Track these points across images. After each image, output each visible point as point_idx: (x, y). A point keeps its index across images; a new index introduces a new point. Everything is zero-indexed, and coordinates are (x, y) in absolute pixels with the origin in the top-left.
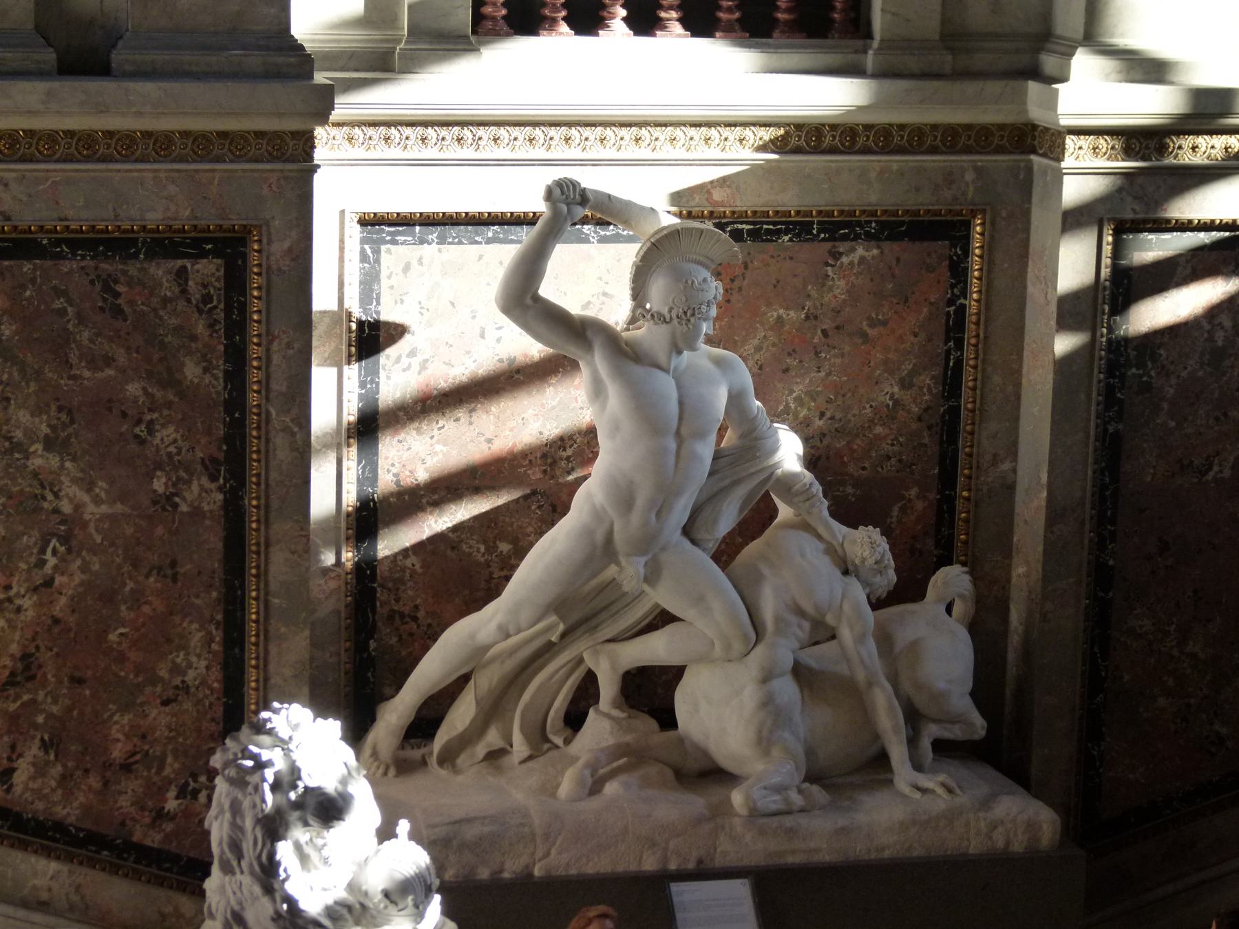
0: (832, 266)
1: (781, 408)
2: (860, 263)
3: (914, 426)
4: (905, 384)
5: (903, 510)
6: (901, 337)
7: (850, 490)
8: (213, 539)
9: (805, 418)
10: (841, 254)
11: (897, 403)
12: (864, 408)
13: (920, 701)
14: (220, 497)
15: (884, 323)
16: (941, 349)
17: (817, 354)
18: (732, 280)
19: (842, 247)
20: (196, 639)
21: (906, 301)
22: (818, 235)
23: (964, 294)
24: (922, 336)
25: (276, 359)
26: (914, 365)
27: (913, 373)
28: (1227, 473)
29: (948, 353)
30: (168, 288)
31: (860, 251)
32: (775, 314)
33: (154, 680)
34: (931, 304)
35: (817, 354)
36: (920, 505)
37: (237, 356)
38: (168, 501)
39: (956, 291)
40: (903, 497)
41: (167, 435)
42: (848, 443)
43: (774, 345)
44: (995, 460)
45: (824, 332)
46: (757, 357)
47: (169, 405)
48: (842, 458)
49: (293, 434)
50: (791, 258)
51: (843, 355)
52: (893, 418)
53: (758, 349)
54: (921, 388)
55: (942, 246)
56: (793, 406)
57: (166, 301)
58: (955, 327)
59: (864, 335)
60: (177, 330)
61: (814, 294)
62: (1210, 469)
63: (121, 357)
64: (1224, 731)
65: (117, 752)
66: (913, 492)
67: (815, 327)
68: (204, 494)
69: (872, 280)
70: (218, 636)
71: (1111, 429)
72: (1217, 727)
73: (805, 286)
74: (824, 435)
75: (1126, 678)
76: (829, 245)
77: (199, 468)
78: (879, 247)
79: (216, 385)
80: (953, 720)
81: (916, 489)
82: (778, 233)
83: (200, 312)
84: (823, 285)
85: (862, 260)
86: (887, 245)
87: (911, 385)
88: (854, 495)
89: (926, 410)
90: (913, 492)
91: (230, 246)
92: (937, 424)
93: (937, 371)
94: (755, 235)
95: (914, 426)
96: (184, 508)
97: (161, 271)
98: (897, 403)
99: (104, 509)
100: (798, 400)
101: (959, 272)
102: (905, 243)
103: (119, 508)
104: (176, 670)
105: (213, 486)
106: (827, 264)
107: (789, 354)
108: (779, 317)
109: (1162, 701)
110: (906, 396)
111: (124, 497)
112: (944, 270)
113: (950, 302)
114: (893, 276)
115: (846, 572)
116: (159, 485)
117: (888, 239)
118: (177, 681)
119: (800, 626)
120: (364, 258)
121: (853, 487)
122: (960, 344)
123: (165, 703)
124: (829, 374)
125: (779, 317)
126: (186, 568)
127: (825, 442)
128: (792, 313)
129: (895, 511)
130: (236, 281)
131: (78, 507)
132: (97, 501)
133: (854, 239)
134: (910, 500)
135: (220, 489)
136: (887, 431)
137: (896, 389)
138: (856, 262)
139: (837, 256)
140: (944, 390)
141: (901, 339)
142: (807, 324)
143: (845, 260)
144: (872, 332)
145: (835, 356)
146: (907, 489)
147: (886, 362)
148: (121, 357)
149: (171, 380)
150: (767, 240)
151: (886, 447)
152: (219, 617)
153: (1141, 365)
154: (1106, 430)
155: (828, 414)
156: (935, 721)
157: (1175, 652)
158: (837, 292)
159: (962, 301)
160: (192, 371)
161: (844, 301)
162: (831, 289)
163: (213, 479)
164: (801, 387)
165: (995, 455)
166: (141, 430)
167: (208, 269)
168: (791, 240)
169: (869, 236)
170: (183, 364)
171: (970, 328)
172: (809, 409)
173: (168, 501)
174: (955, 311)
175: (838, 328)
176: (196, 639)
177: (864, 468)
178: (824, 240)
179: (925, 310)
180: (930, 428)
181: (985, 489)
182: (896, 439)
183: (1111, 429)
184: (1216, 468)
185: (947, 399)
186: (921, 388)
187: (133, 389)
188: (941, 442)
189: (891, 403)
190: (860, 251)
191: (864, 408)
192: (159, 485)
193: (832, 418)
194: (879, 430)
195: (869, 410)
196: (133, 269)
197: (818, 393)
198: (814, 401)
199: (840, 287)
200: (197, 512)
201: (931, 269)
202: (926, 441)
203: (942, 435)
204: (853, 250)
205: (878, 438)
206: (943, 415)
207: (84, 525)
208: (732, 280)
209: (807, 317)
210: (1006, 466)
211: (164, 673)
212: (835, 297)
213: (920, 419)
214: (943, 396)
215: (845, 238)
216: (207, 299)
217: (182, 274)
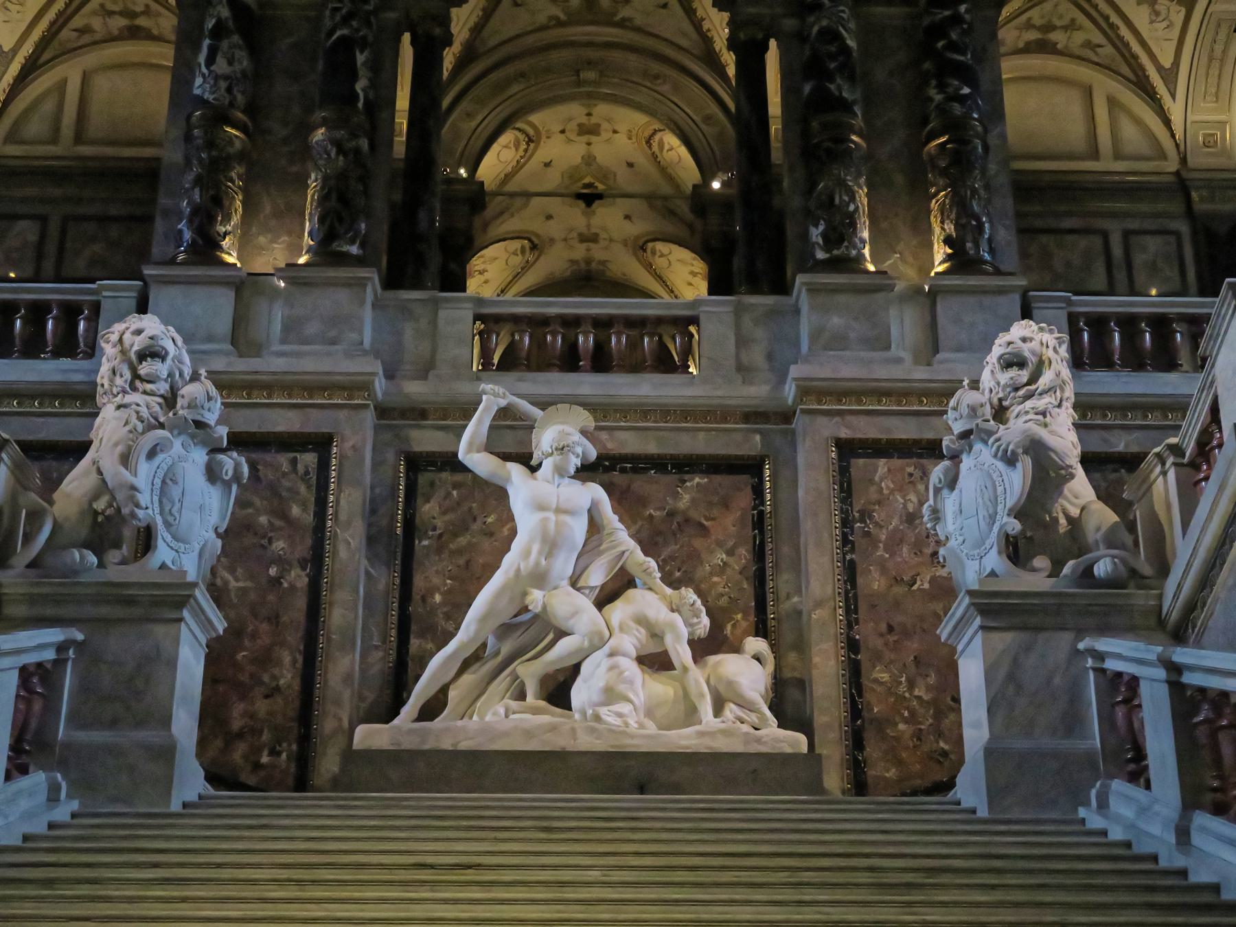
4: (730, 553)
5: (734, 626)
8: (301, 602)
11: (725, 563)
13: (722, 689)
14: (306, 580)
15: (713, 519)
16: (750, 534)
17: (675, 535)
19: (686, 477)
20: (287, 659)
23: (763, 503)
25: (343, 502)
27: (735, 546)
28: (926, 586)
30: (286, 467)
31: (697, 480)
33: (262, 683)
36: (744, 624)
37: (321, 503)
38: (276, 582)
41: (279, 545)
44: (788, 597)
47: (280, 529)
49: (349, 544)
55: (745, 479)
57: (284, 475)
58: (759, 522)
59: (702, 525)
60: (289, 490)
62: (915, 583)
63: (257, 502)
64: (946, 747)
65: (236, 724)
66: (739, 616)
68: (298, 578)
70: (300, 659)
71: (848, 557)
72: (942, 744)
75: (876, 710)
76: (677, 476)
77: (295, 563)
79: (309, 519)
83: (303, 480)
85: (698, 484)
86: (713, 476)
90: (739, 616)
91: (322, 443)
93: (750, 546)
94: (635, 470)
96: (286, 585)
97: (283, 460)
98: (725, 563)
99: (241, 584)
101: (758, 492)
103: (249, 584)
104: (274, 677)
105: (303, 574)
108: (651, 515)
109: (901, 727)
110: (731, 560)
111: (251, 577)
112: (749, 490)
115: (673, 611)
116: (273, 571)
118: (274, 684)
120: (408, 478)
122: (762, 532)
123: (267, 697)
124: (682, 546)
126: (285, 619)
129: (729, 627)
130: (324, 465)
131: (226, 583)
132: (237, 580)
135: (308, 575)
148: (257, 502)
149: (284, 515)
151: (721, 590)
152: (302, 648)
153: (862, 521)
154: (844, 558)
157: (907, 695)
160: (295, 511)
163: (304, 569)
166: (265, 542)
167: (309, 459)
170: (291, 507)
171: (767, 521)
173: (276, 582)
176: (287, 659)
183: (848, 557)
184: (919, 583)
187: (263, 519)
190: (697, 480)
192: (273, 571)
196: (268, 457)
199: (687, 497)
200: (292, 588)
201: (739, 489)
205: (716, 583)
207: (228, 591)
210: (796, 599)
211: (266, 678)
213: (740, 573)
215: (687, 472)
216: (307, 473)
217: (294, 462)
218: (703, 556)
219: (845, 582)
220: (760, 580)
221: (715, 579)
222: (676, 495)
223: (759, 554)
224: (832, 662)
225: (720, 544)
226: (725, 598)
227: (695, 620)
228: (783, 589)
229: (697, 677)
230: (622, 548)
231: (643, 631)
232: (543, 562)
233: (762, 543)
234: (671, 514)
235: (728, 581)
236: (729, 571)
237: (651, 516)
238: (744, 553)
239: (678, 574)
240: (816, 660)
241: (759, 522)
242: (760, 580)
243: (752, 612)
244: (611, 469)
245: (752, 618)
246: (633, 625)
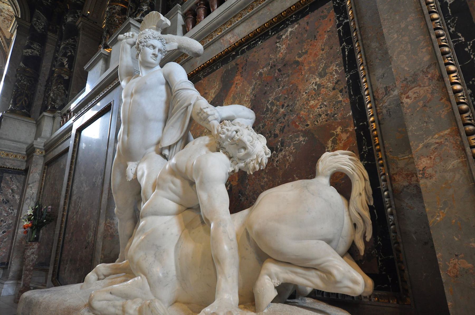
0: (279, 42)
1: (265, 109)
2: (290, 34)
3: (331, 94)
6: (315, 54)
7: (301, 139)
9: (276, 110)
10: (282, 36)
11: (319, 86)
12: (303, 95)
15: (306, 53)
16: (339, 49)
17: (277, 80)
18: (242, 68)
21: (315, 37)
22: (272, 34)
24: (327, 47)
26: (325, 64)
29: (343, 50)
32: (259, 73)
34: (328, 32)
35: (277, 80)
36: (344, 136)
39: (341, 19)
40: (333, 134)
42: (297, 115)
43: (259, 85)
45: (279, 70)
46: (254, 92)
48: (295, 123)
50: (262, 49)
51: (288, 76)
52: (318, 95)
53: (253, 89)
54: (331, 73)
56: (269, 107)
59: (297, 63)
61: (273, 57)
66: (339, 130)
67: (275, 69)
69: (297, 38)
73: (269, 56)
74: (285, 115)
78: (297, 24)
80: (307, 265)
81: (339, 127)
82: (257, 43)
84: (276, 51)
85: (291, 32)
86: (301, 21)
87: (326, 74)
88: (304, 141)
89: (336, 83)
90: (339, 130)
92: (345, 88)
93: (340, 60)
95: (331, 94)
100: (272, 104)
102: (310, 14)
106: (277, 43)
107: (266, 86)
113: (338, 26)
114: (306, 31)
117: (301, 18)
119: (173, 182)
121: (303, 136)
122: (350, 42)
124: (283, 87)
125: (260, 73)
127: (286, 118)
128: (265, 69)
133: (287, 27)
134: (337, 135)
136: (317, 101)
137: (318, 79)
138: (288, 34)
139: (279, 38)
140: (345, 69)
141: (316, 55)
142: (272, 70)
143: (284, 37)
144: (300, 60)
145: (286, 77)
146: (335, 129)
147: (310, 69)
150: (253, 47)
155: (286, 105)
156: (277, 261)
158: (282, 51)
159: (346, 21)
161: (286, 53)
162: (280, 51)
164: (272, 97)
165: (386, 88)
168: (261, 42)
169: (293, 22)
172: (277, 106)
174: (342, 28)
175: (285, 65)
177: (307, 125)
178: (274, 35)
179: (326, 36)
180: (341, 91)
181: (384, 111)
182: (322, 104)
185: (349, 72)
186: (331, 73)
188: (350, 96)
189: (316, 87)
190: (290, 30)
191: (303, 95)
193: (288, 106)
194: (312, 103)
195: (305, 95)
197: (280, 97)
198: (279, 101)
199: (283, 48)
202: (341, 99)
203: (350, 93)
204: (287, 31)
205: (312, 107)
206: (348, 81)
208: (242, 68)
209: (271, 67)
212: (282, 53)
213: (334, 89)
214: (346, 72)
218: (300, 87)
219: (453, 36)
220: (354, 87)
221: (312, 103)
222: (275, 50)
223: (350, 63)
224: (454, 162)
225: (311, 71)
226: (323, 116)
227: (243, 152)
228: (380, 86)
229: (227, 226)
230: (185, 105)
231: (178, 181)
232: (126, 138)
233: (352, 51)
234: (273, 66)
235: (323, 99)
236: (323, 90)
237: (261, 74)
238: (336, 69)
239: (282, 110)
240: (423, 163)
241: (345, 35)
242: (354, 87)
243: (352, 122)
244: (237, 54)
245: (351, 129)
246: (169, 178)
